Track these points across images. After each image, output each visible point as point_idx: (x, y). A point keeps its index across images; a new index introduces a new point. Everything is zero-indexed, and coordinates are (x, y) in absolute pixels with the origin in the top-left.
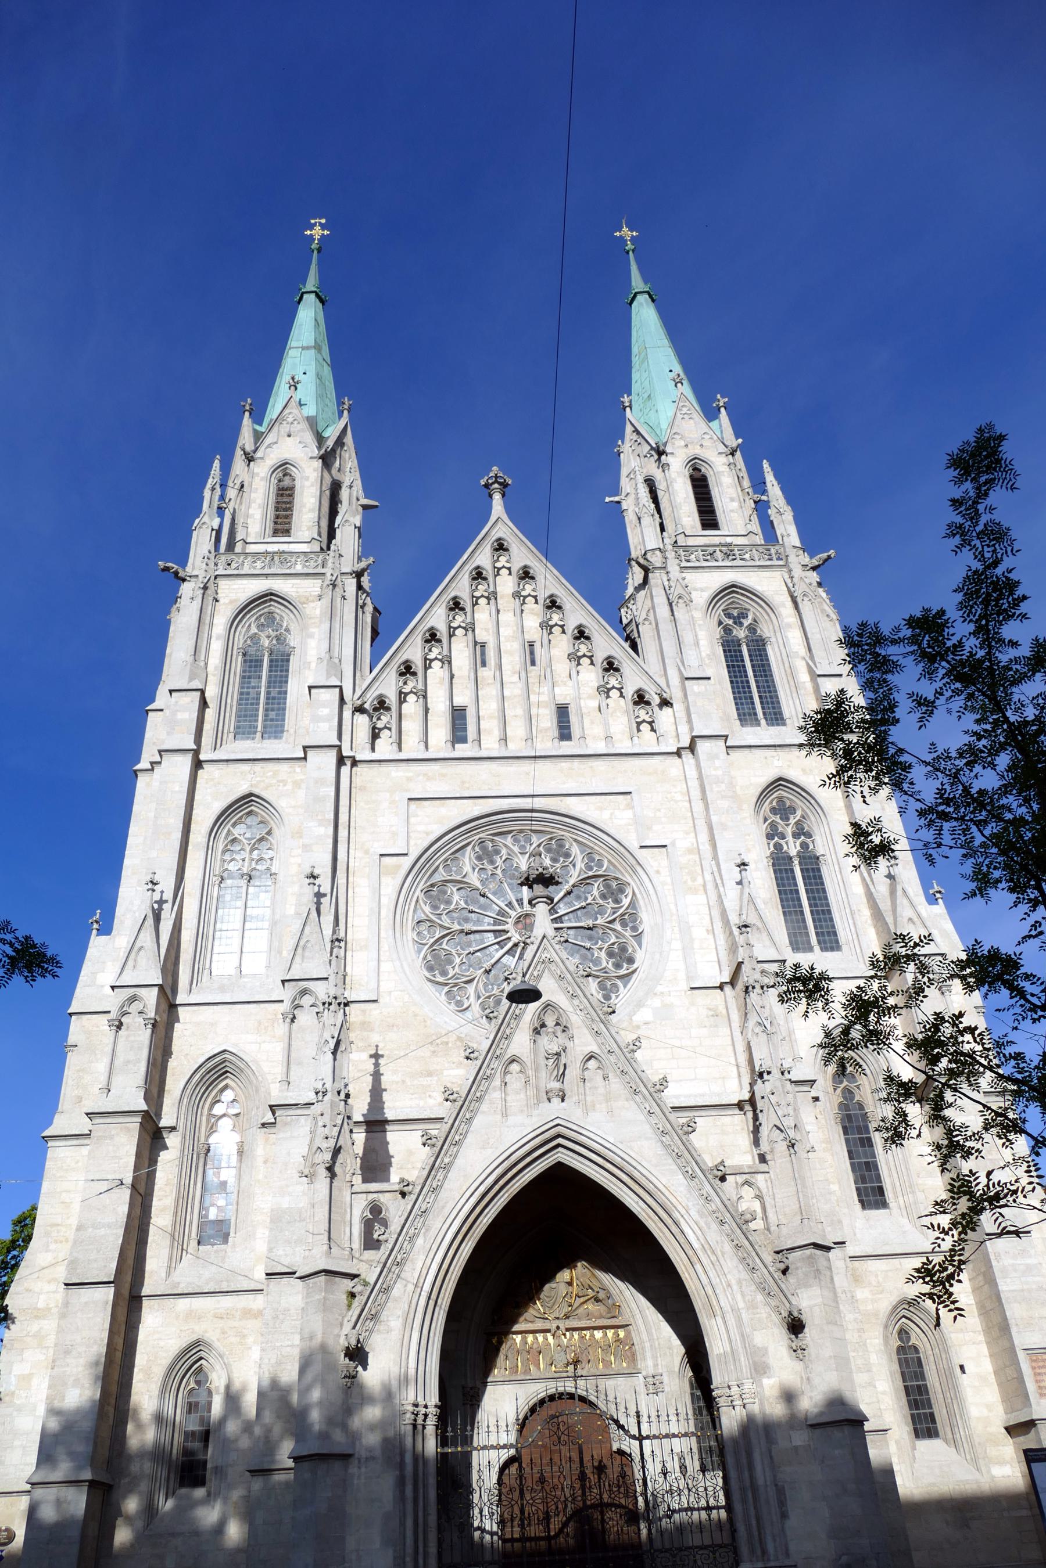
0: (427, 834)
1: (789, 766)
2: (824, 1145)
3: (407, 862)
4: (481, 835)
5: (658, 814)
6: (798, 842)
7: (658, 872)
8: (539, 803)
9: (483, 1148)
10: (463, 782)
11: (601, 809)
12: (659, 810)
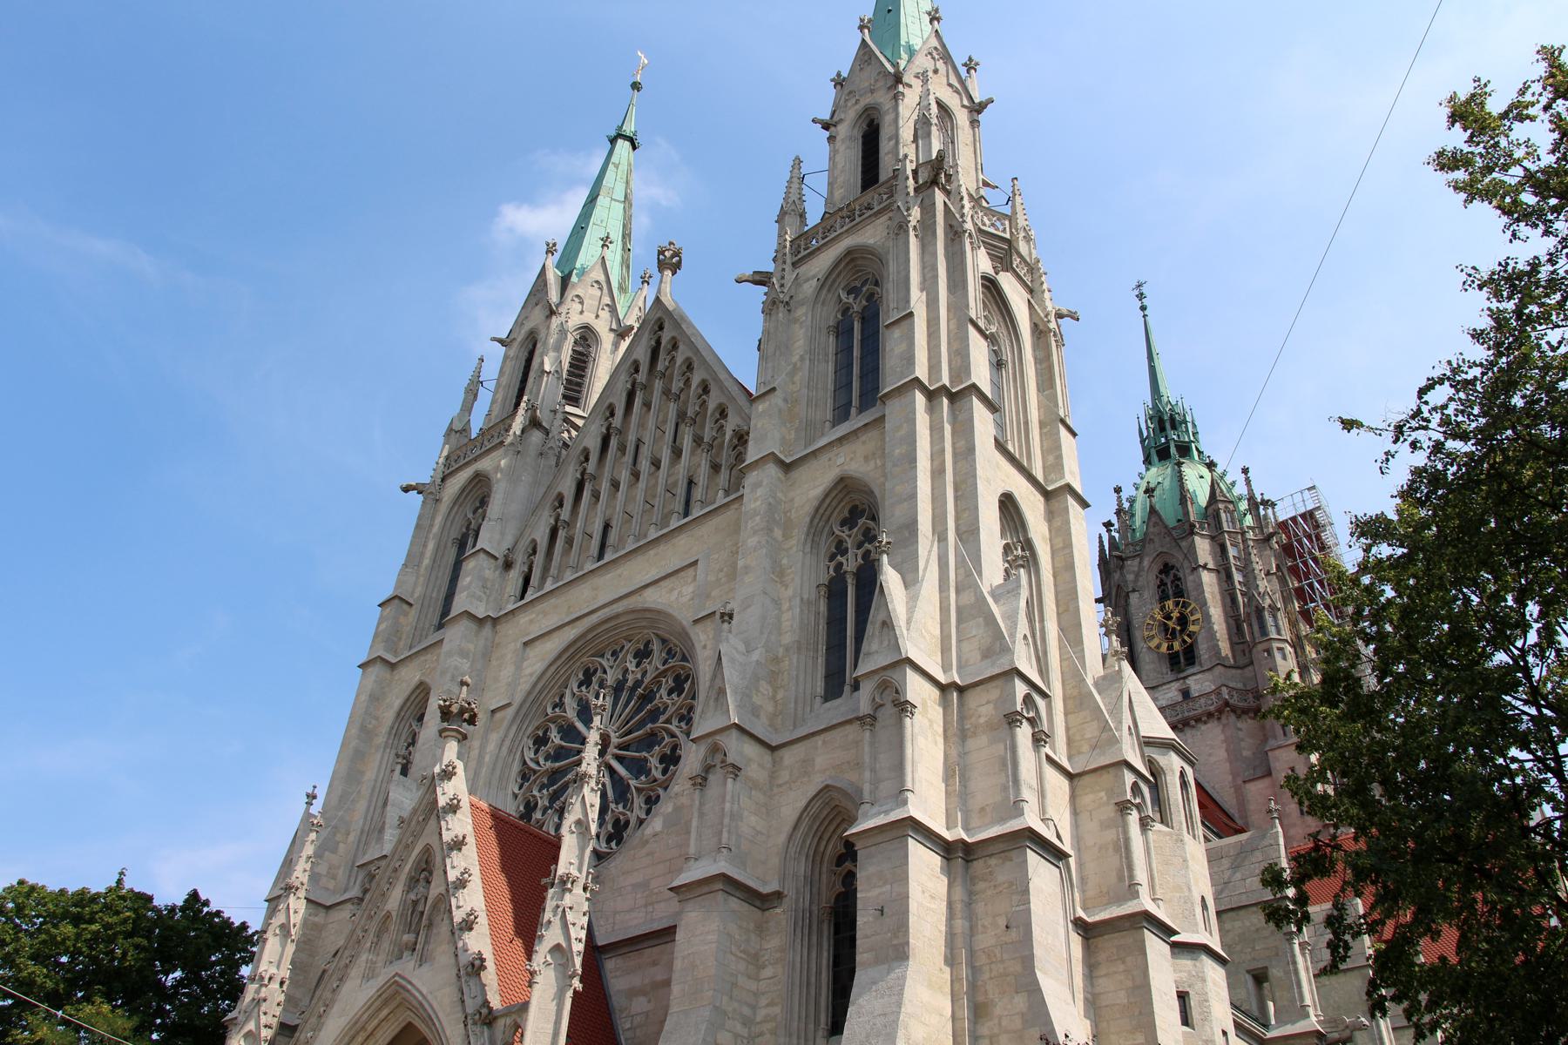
0: (531, 675)
1: (851, 459)
2: (778, 955)
3: (510, 711)
4: (585, 659)
5: (721, 575)
6: (860, 552)
7: (705, 647)
8: (619, 608)
9: (340, 1017)
10: (569, 607)
11: (672, 590)
12: (721, 570)
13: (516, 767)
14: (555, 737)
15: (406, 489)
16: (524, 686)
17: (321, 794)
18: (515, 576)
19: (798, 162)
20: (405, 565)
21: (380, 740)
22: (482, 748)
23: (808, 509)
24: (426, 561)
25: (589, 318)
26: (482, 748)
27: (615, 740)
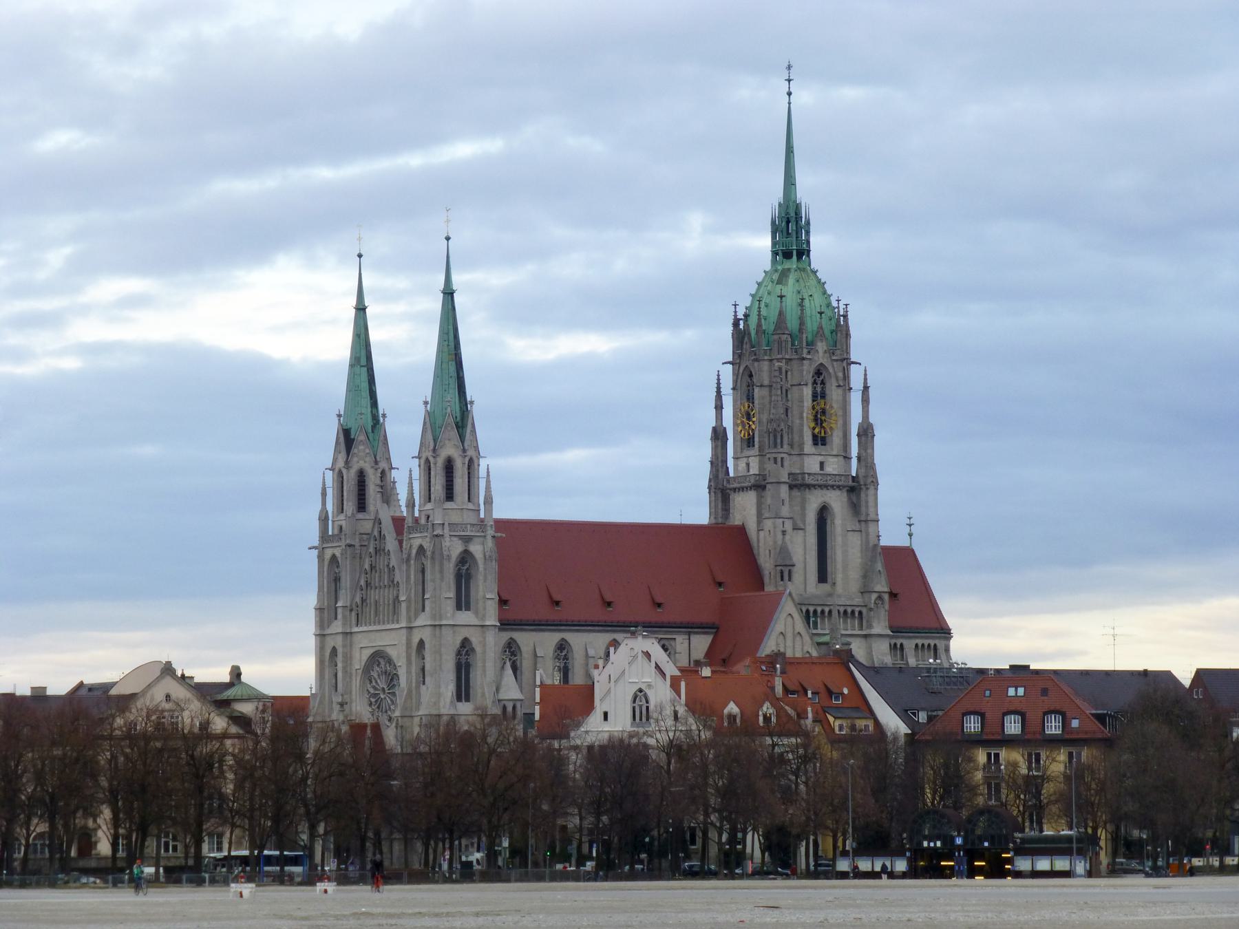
8: (382, 648)
13: (366, 689)
14: (374, 681)
15: (310, 548)
16: (363, 664)
17: (314, 686)
18: (354, 614)
19: (411, 471)
20: (319, 591)
21: (327, 664)
22: (356, 680)
23: (416, 644)
24: (325, 590)
25: (362, 464)
26: (356, 680)
27: (387, 691)
